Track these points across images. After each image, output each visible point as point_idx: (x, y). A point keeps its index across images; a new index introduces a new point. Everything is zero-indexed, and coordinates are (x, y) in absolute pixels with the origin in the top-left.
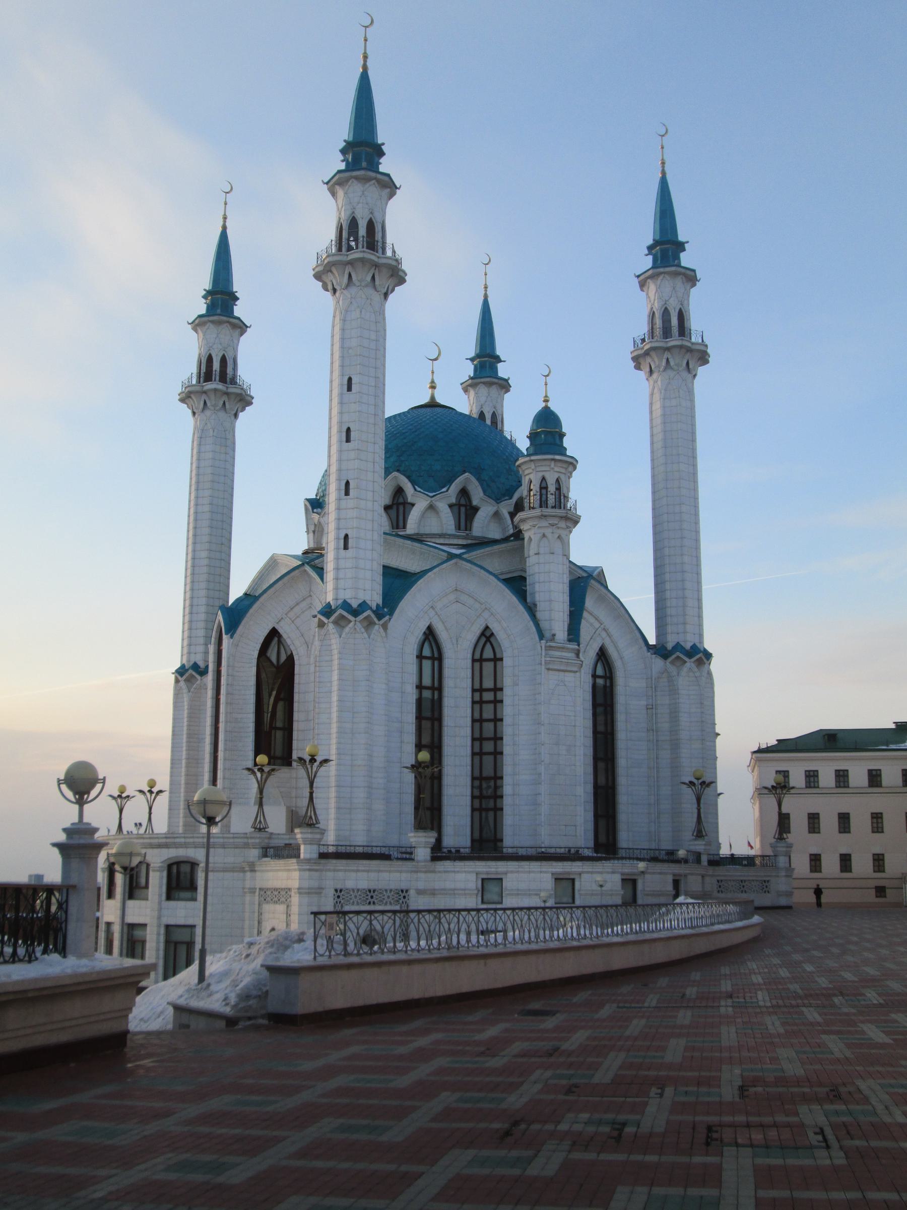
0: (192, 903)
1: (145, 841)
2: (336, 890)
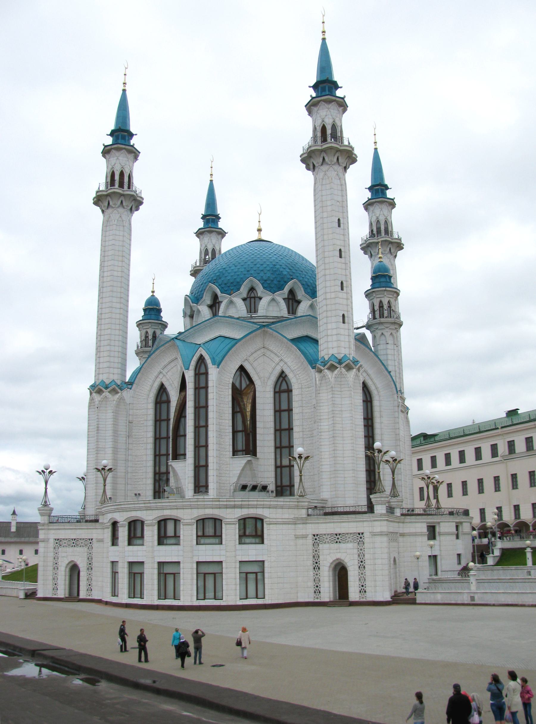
0: (261, 545)
1: (221, 503)
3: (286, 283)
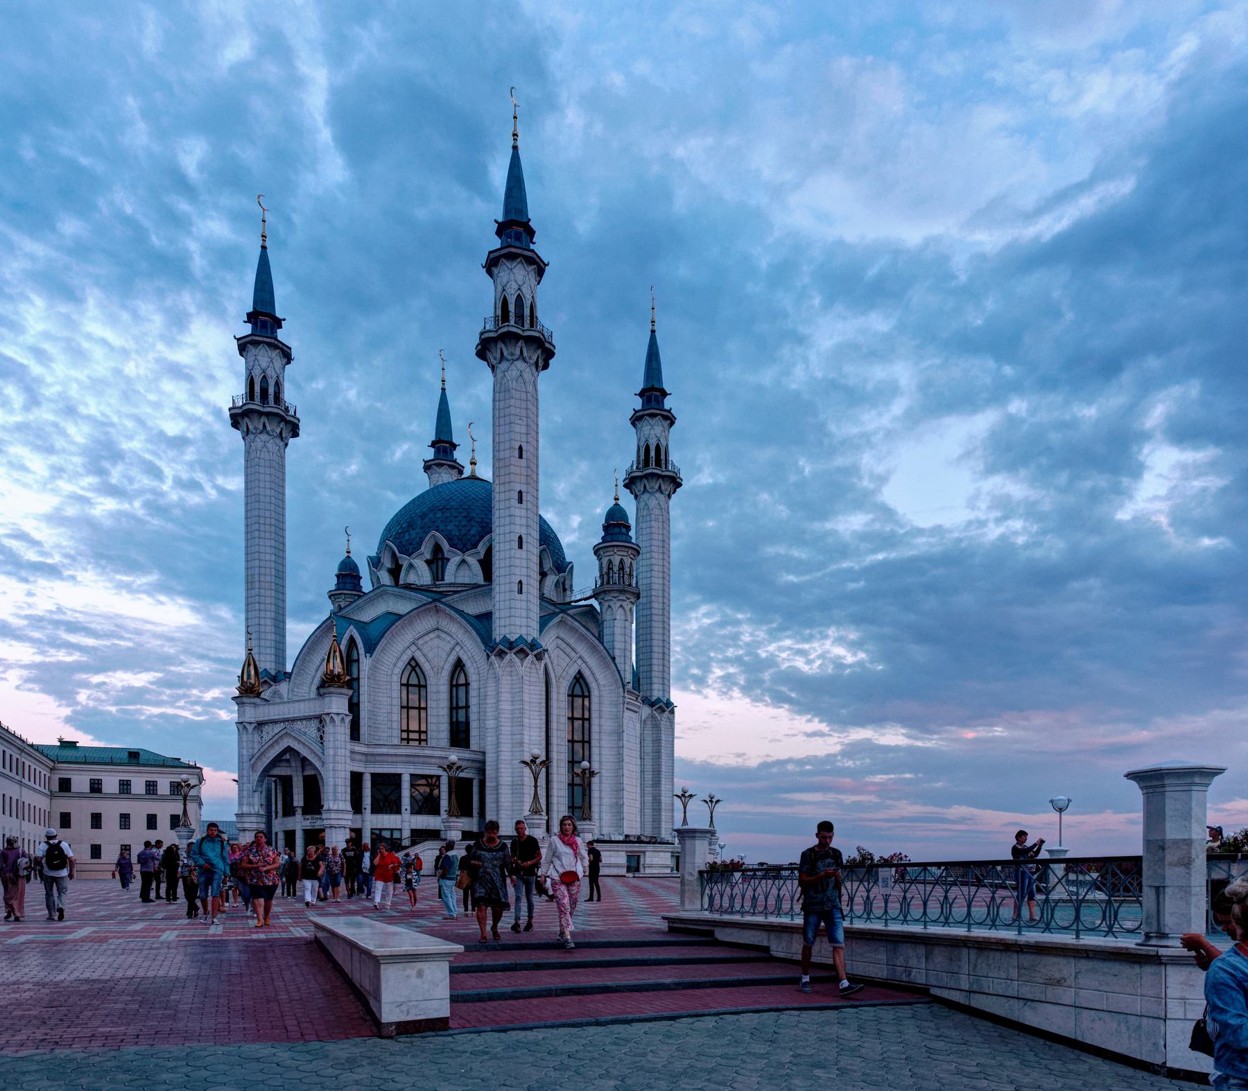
3: (482, 537)
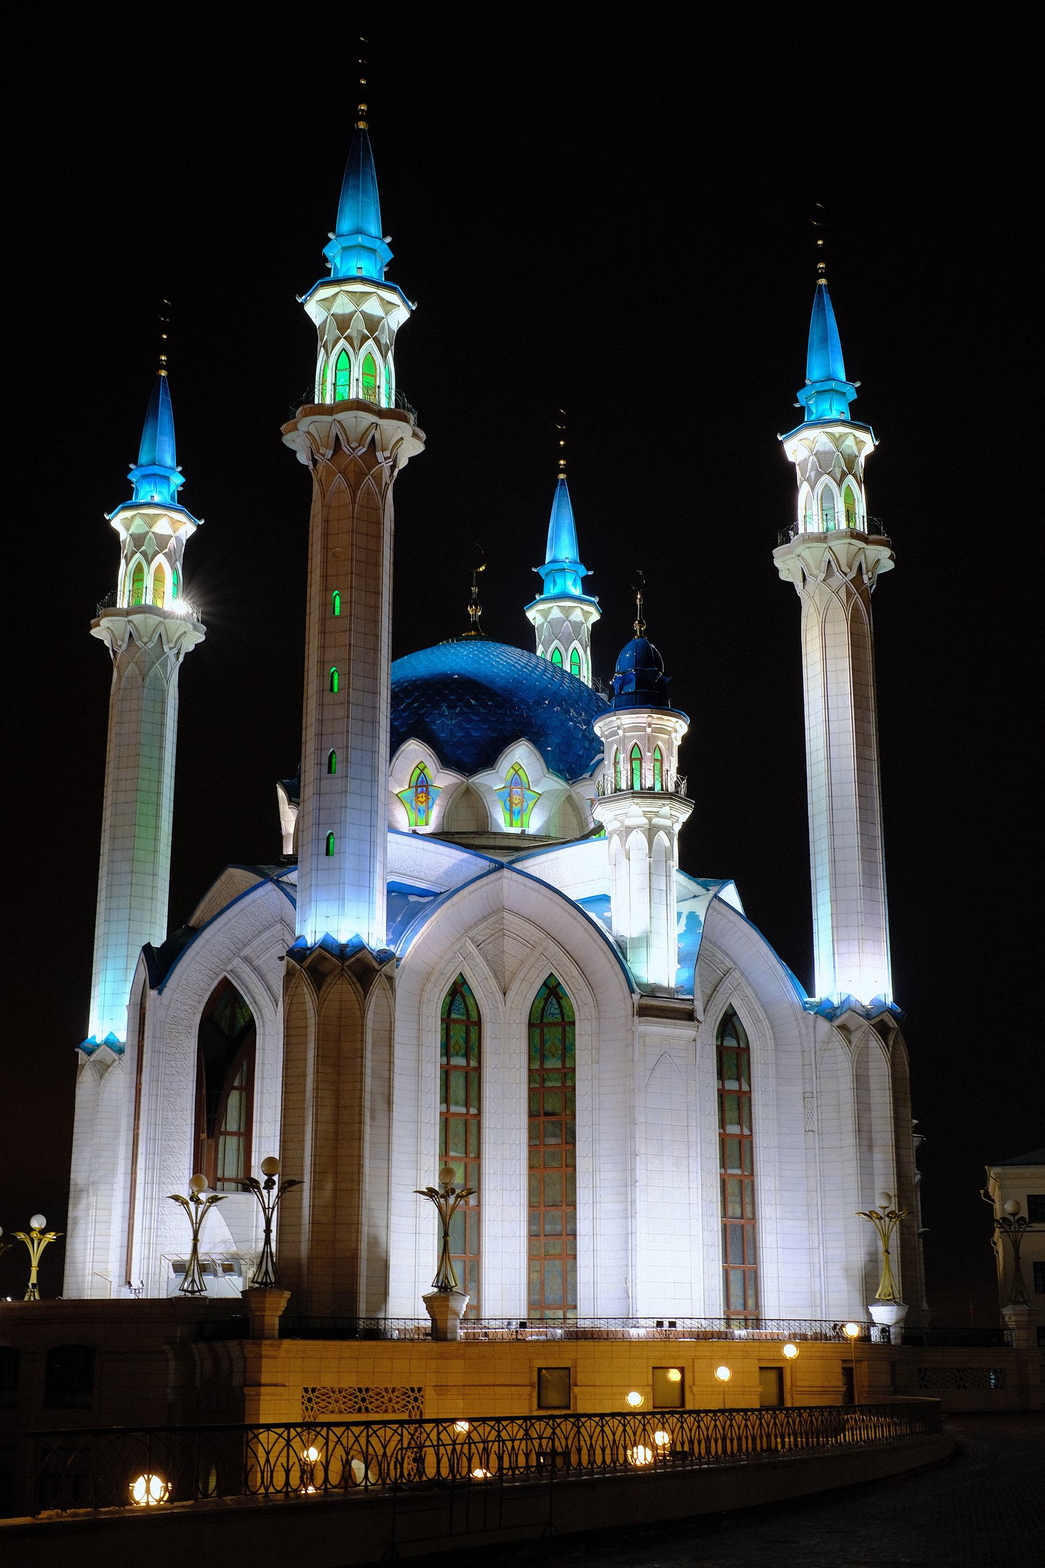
2: (306, 1390)
